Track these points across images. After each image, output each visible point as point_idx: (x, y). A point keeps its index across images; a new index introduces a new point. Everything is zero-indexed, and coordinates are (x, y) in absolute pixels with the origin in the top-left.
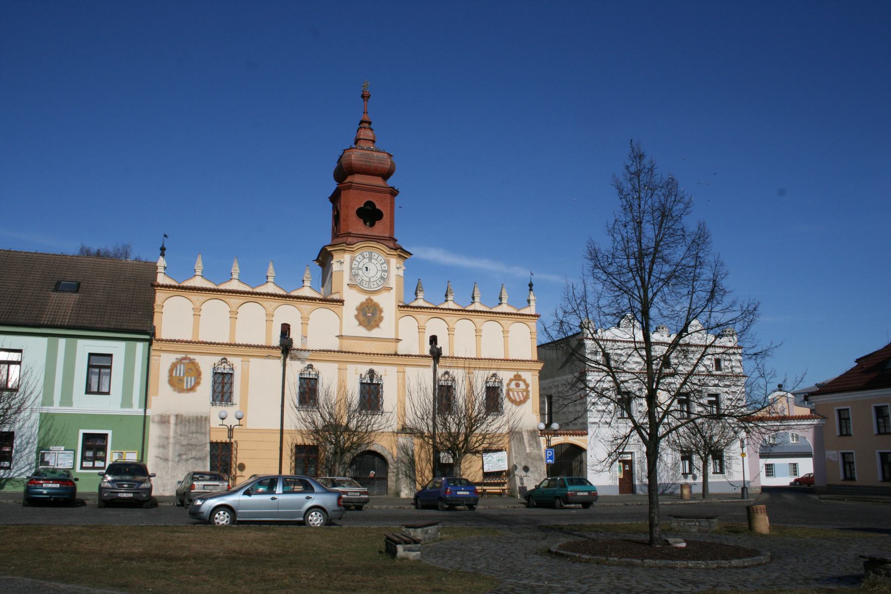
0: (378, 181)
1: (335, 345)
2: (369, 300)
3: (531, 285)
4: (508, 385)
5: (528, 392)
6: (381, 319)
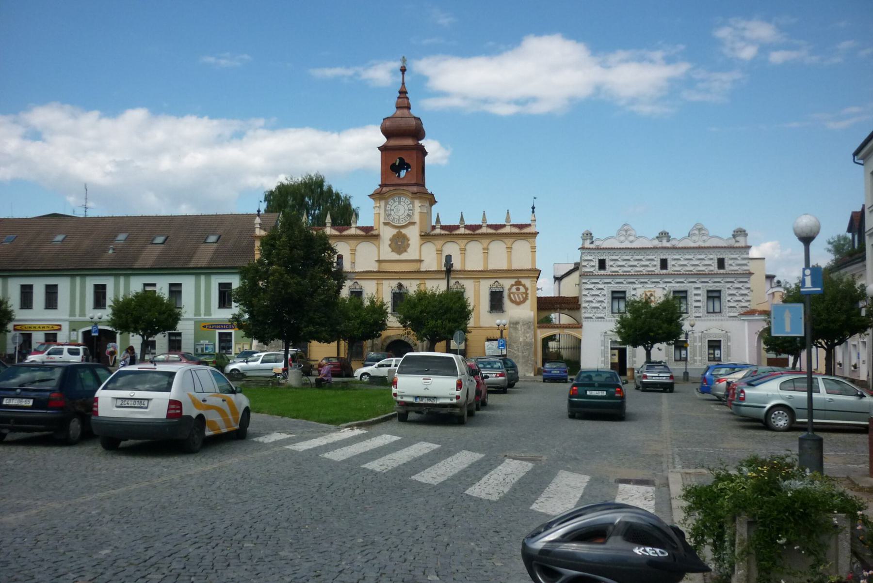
0: (409, 142)
1: (374, 267)
2: (399, 233)
3: (533, 208)
4: (510, 289)
5: (527, 294)
6: (408, 245)
